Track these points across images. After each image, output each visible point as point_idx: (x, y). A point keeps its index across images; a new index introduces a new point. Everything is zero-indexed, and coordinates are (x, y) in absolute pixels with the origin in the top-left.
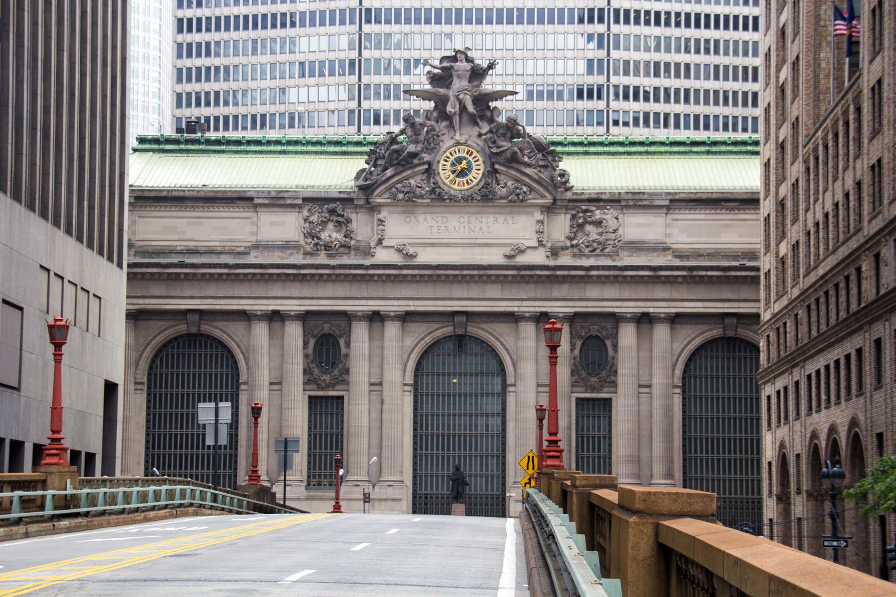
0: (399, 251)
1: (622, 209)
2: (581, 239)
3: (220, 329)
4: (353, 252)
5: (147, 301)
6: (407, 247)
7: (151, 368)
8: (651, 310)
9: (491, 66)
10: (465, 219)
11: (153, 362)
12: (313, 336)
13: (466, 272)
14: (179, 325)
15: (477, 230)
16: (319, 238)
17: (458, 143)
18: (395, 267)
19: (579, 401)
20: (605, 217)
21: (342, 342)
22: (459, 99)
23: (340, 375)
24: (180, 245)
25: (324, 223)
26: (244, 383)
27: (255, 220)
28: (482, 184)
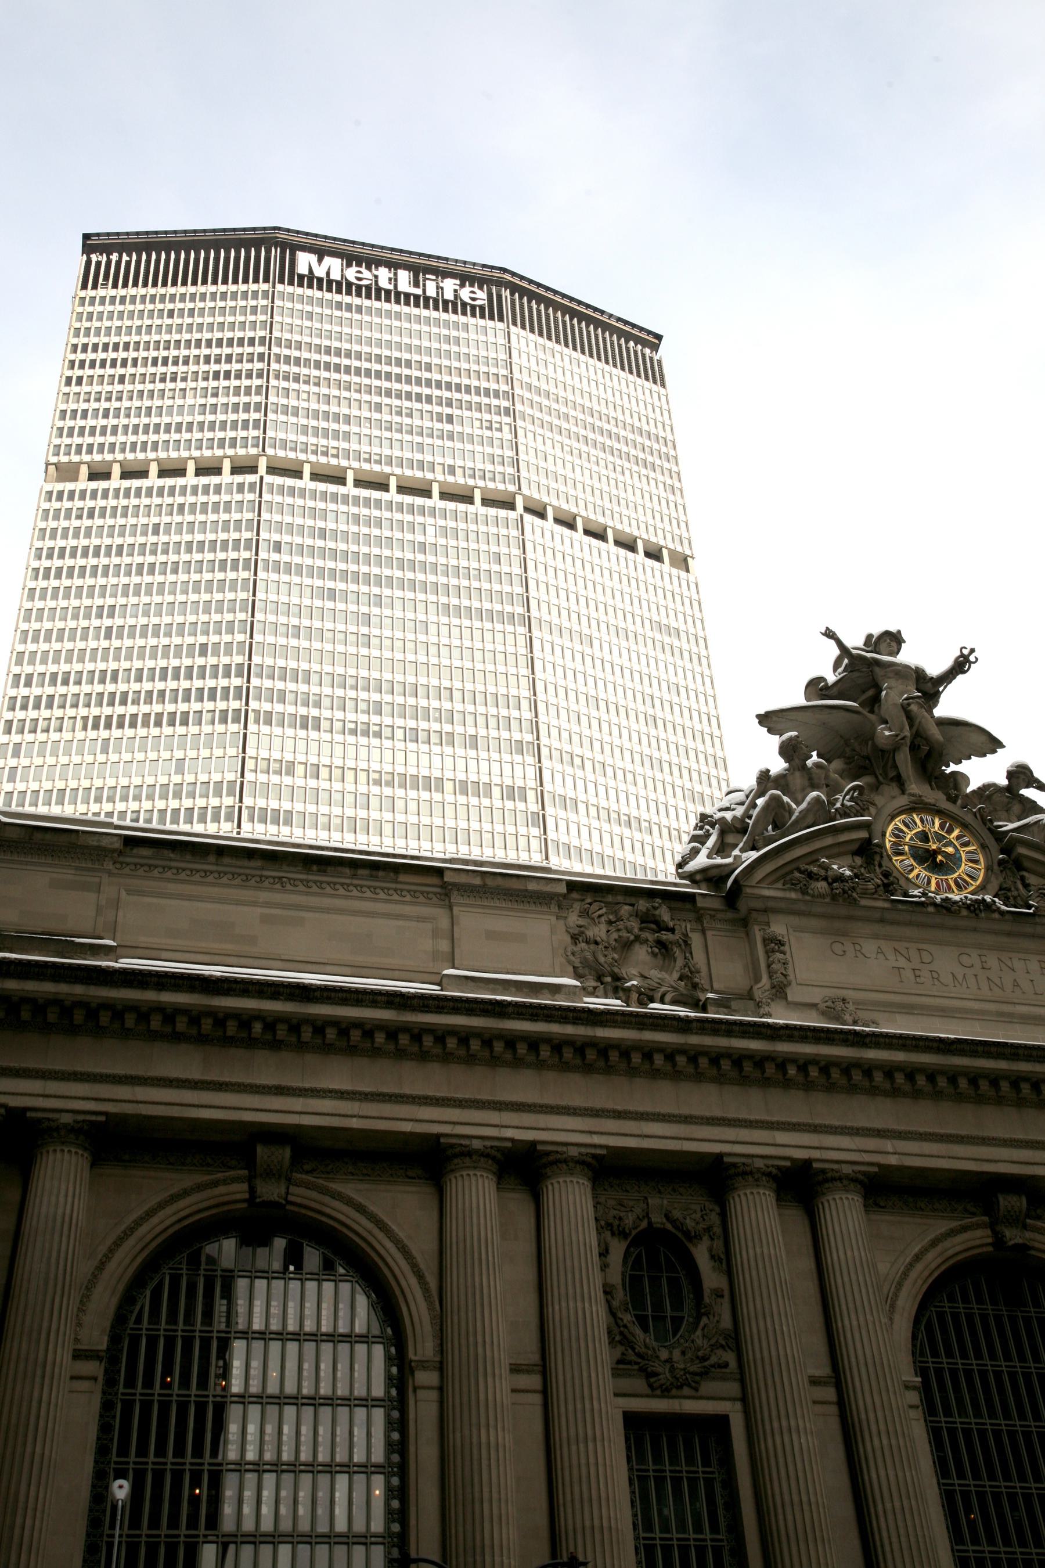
3: (349, 1202)
5: (142, 1093)
6: (851, 1007)
7: (120, 1319)
9: (961, 665)
10: (974, 958)
11: (128, 1299)
12: (623, 1234)
13: (1024, 1067)
14: (225, 1182)
16: (617, 978)
17: (918, 806)
21: (701, 1254)
22: (910, 717)
23: (714, 1347)
25: (626, 946)
26: (424, 1365)
27: (444, 923)
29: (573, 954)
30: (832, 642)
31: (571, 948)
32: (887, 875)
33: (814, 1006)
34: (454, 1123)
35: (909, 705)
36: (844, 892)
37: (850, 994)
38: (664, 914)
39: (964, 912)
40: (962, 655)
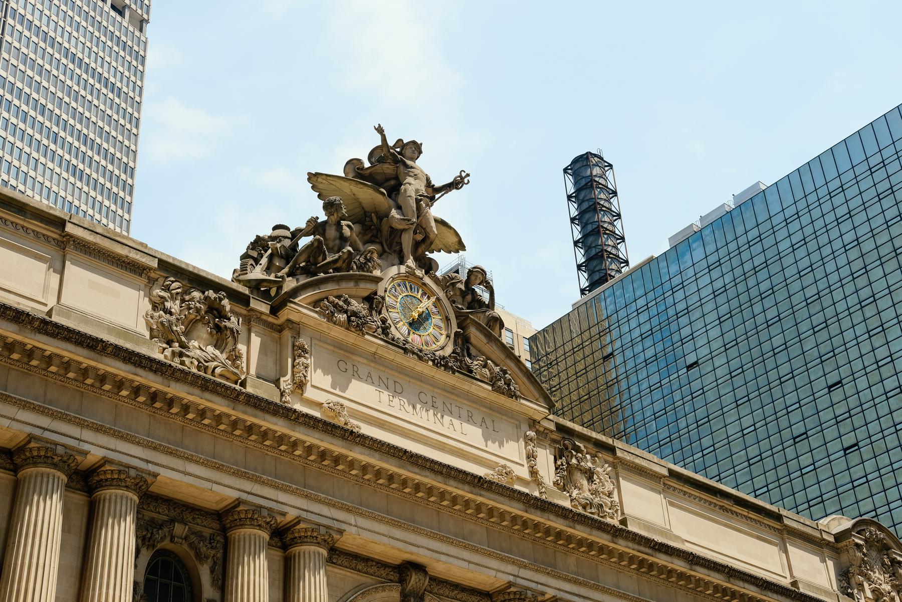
1: (614, 466)
9: (456, 184)
16: (183, 345)
21: (205, 574)
29: (152, 317)
30: (379, 136)
31: (151, 312)
32: (384, 321)
33: (319, 405)
34: (45, 429)
35: (421, 200)
36: (358, 325)
37: (346, 403)
39: (430, 363)
40: (460, 176)
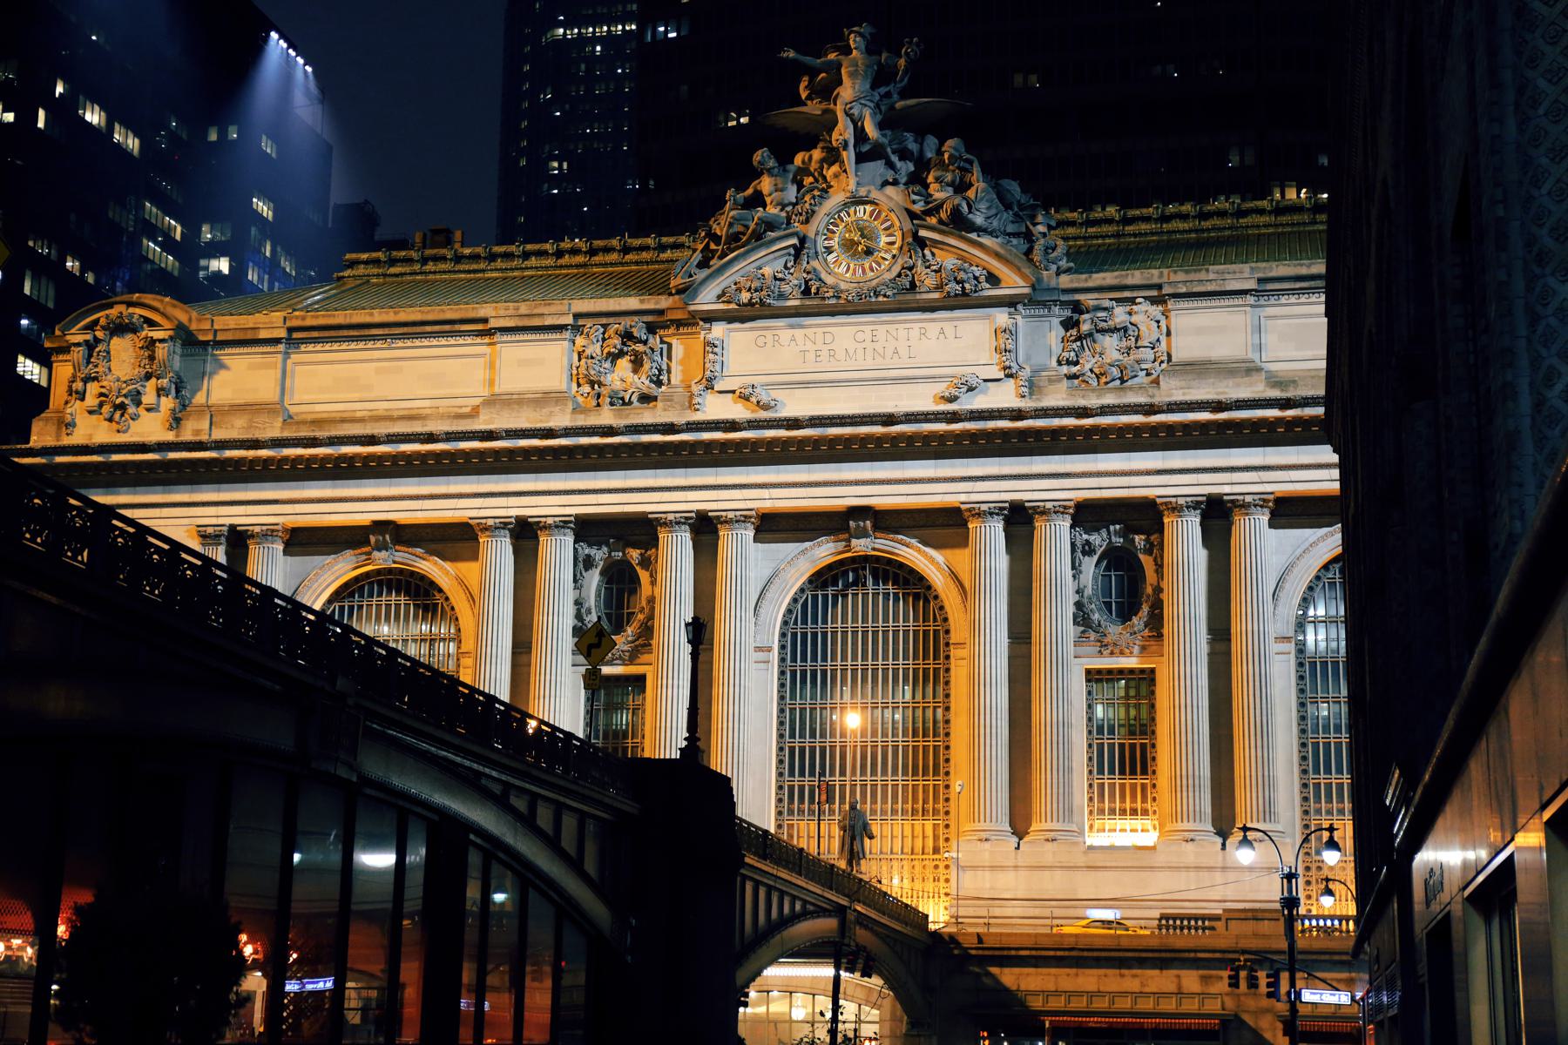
0: (745, 398)
2: (1088, 363)
4: (660, 404)
8: (1227, 489)
15: (889, 352)
16: (600, 384)
18: (732, 426)
19: (1088, 672)
20: (1134, 319)
24: (361, 409)
25: (614, 357)
28: (896, 269)
38: (639, 332)
